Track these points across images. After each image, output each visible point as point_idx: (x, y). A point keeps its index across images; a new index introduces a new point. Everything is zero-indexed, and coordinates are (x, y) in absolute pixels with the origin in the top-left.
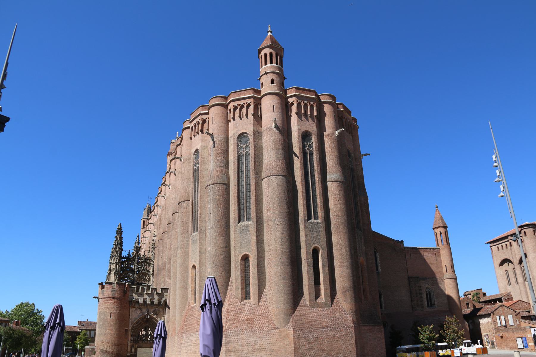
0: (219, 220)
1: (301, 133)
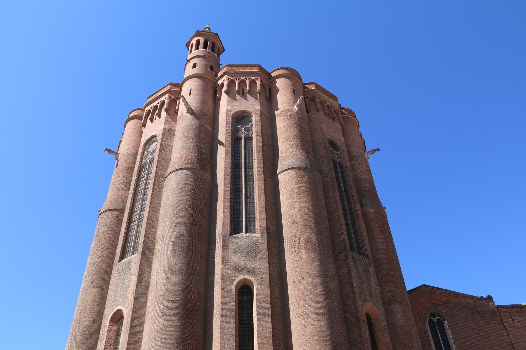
0: (97, 262)
1: (231, 114)
